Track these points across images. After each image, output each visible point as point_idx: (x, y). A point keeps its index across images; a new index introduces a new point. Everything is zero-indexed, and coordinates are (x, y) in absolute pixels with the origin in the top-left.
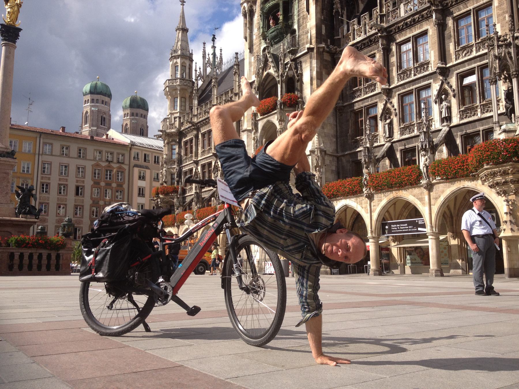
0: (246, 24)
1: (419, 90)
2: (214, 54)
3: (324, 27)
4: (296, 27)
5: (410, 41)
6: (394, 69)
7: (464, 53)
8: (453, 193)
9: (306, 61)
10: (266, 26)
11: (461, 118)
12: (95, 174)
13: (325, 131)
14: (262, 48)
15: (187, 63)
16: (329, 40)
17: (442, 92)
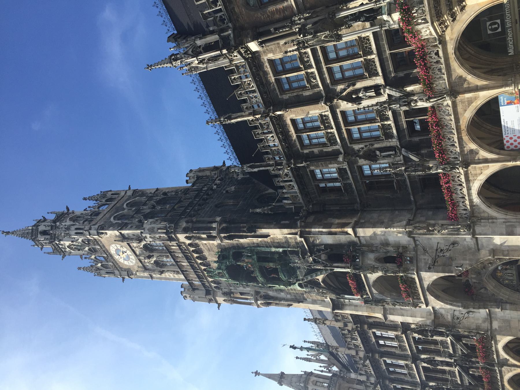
0: (276, 304)
1: (347, 123)
2: (308, 349)
3: (283, 222)
4: (281, 250)
5: (300, 136)
6: (325, 150)
7: (313, 80)
8: (462, 65)
10: (278, 281)
11: (377, 75)
13: (386, 221)
15: (313, 378)
16: (295, 218)
17: (349, 98)
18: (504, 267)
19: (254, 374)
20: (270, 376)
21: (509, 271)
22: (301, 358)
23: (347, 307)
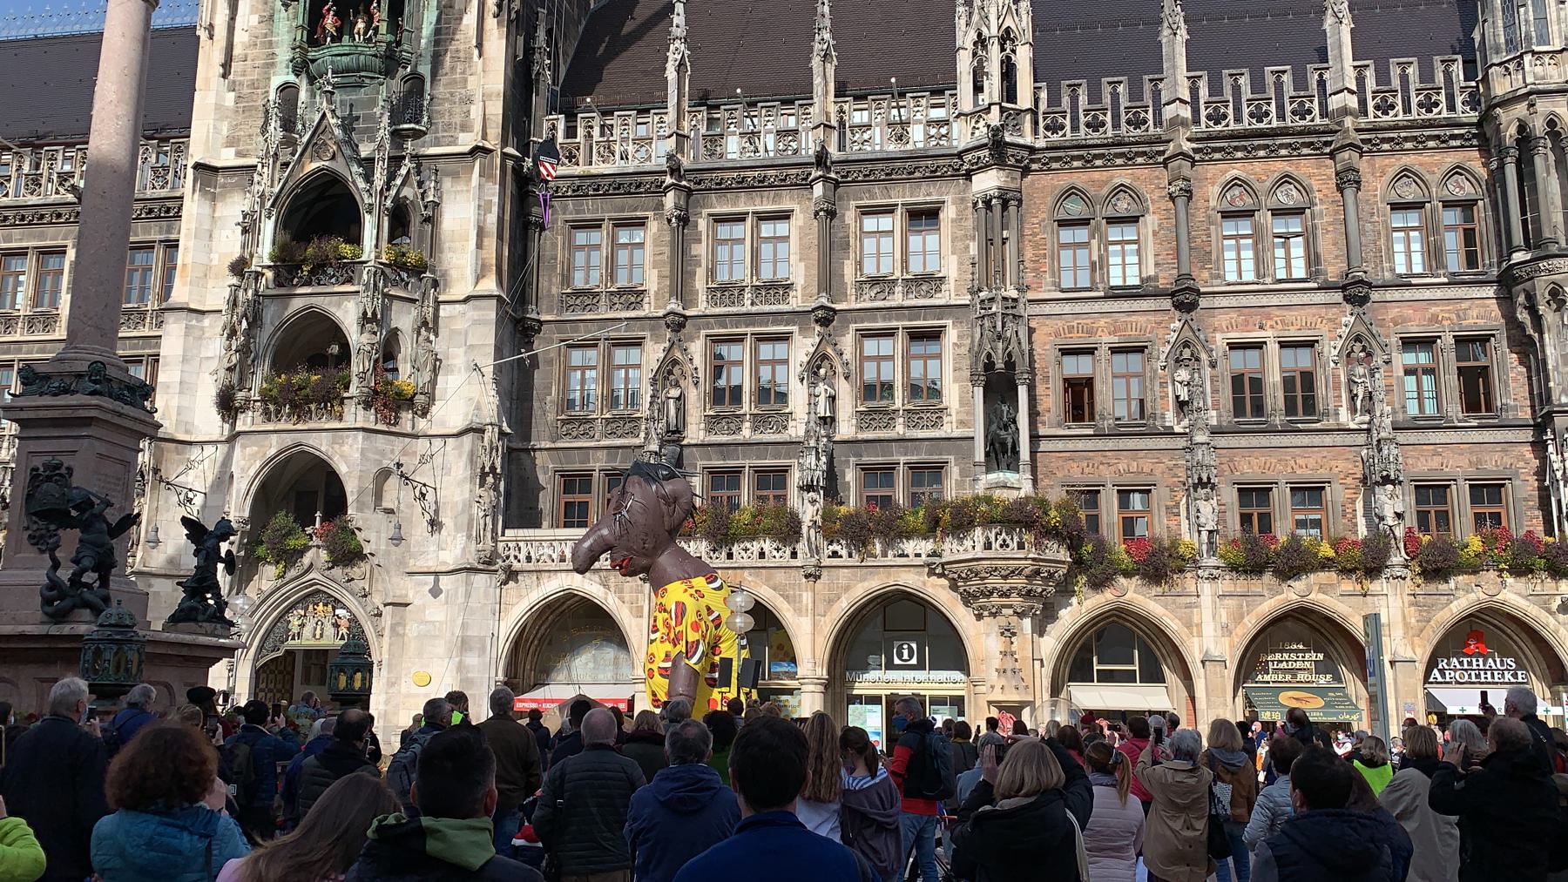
4: (425, 69)
6: (701, 273)
9: (455, 175)
14: (276, 81)
18: (344, 623)
21: (330, 630)
23: (206, 209)
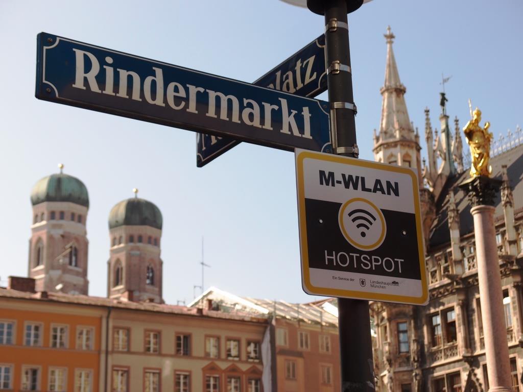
2: (447, 131)
12: (208, 386)
15: (413, 153)
19: (388, 33)
20: (393, 67)
22: (428, 119)
